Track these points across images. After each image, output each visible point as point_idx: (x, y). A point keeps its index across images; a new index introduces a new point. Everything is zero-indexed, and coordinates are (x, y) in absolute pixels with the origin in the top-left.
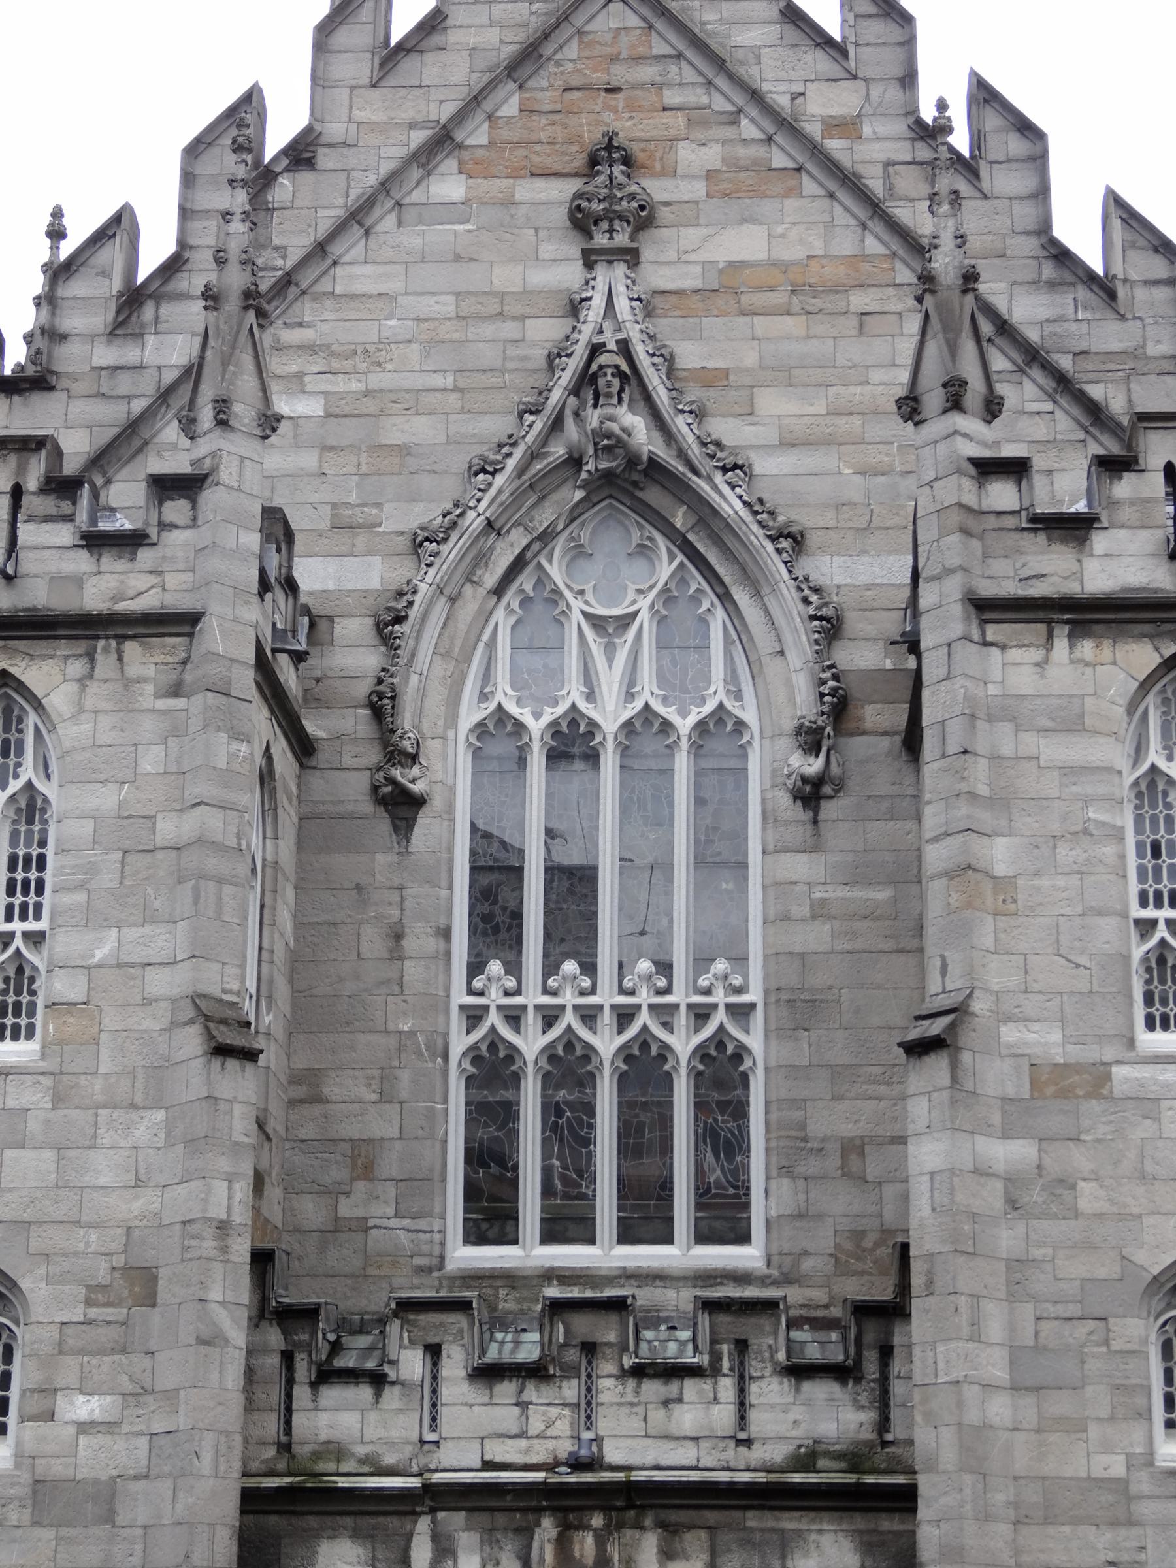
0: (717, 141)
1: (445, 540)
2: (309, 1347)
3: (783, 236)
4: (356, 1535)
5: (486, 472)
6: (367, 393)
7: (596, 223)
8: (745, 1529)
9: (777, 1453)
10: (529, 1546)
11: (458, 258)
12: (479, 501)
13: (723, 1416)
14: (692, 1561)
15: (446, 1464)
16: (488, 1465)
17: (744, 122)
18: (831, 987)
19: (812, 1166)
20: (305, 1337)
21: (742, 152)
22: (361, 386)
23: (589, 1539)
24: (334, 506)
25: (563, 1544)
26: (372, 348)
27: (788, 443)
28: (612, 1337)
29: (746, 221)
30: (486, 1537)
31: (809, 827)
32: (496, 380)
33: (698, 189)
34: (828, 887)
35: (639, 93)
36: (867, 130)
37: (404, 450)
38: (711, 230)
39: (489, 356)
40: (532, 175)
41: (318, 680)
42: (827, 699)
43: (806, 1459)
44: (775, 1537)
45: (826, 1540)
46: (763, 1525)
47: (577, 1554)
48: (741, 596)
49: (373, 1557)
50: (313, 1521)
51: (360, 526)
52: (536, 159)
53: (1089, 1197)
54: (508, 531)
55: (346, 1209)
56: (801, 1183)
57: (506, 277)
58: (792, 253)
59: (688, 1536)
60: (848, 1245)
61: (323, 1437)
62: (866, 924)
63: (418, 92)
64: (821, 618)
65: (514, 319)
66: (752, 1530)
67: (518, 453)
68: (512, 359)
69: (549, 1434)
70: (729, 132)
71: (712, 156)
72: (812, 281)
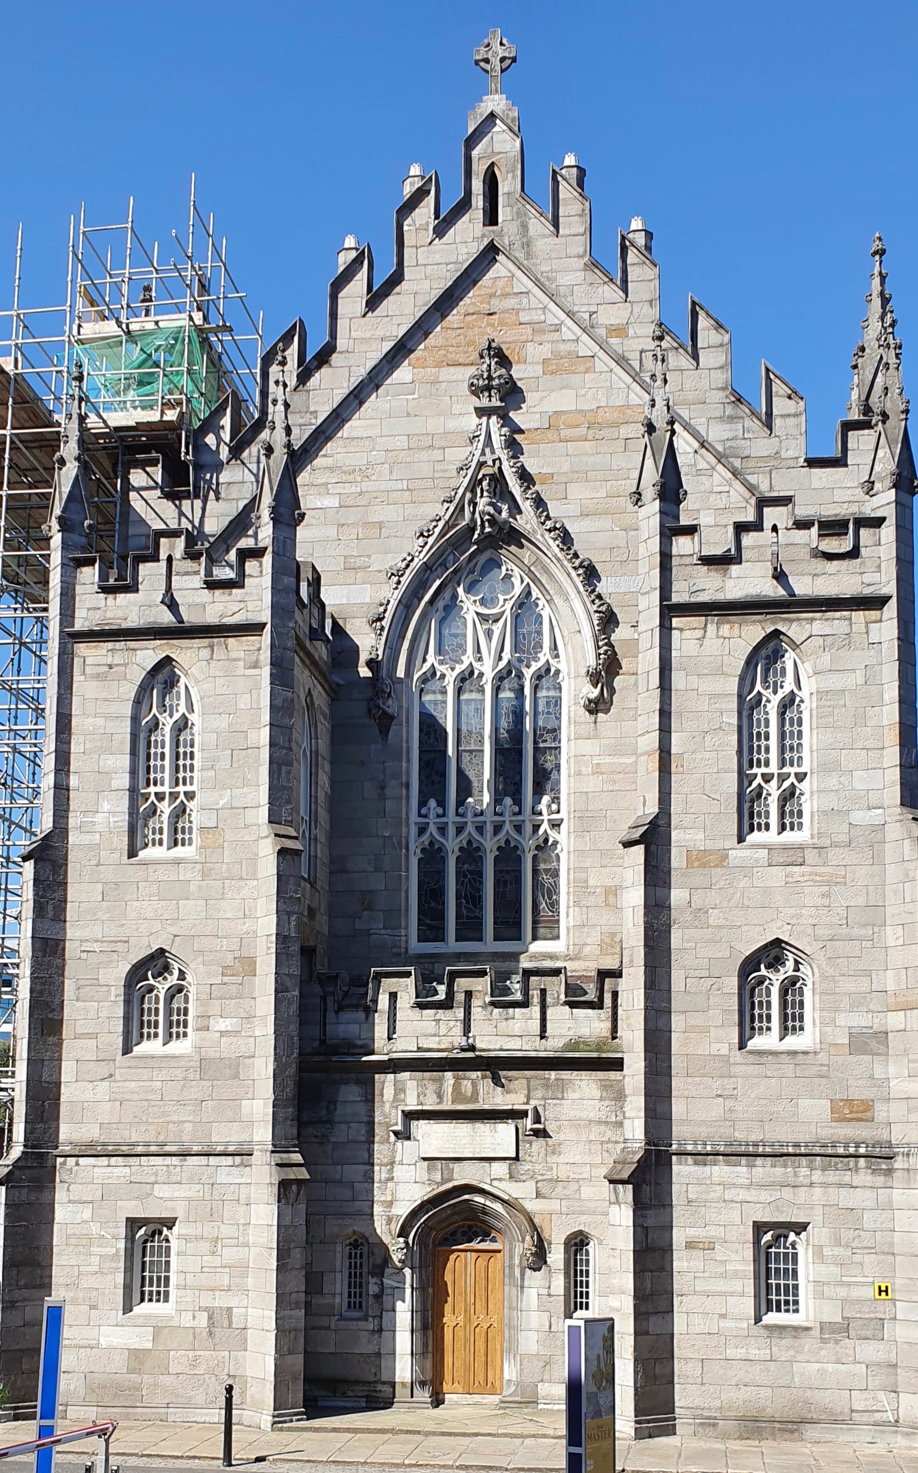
0: (548, 342)
1: (402, 575)
2: (333, 994)
3: (584, 395)
5: (424, 536)
6: (361, 493)
7: (482, 392)
9: (559, 1043)
11: (408, 415)
12: (420, 552)
13: (535, 1026)
15: (400, 1049)
16: (420, 1049)
17: (564, 329)
18: (601, 810)
19: (592, 900)
20: (331, 989)
21: (562, 347)
22: (359, 490)
24: (345, 557)
25: (456, 1087)
26: (364, 468)
27: (584, 515)
28: (480, 988)
29: (564, 387)
31: (593, 725)
32: (430, 484)
33: (539, 369)
34: (602, 757)
35: (507, 315)
36: (631, 332)
37: (381, 525)
38: (545, 394)
39: (426, 470)
40: (448, 365)
41: (339, 653)
42: (602, 656)
43: (573, 1045)
47: (463, 1091)
48: (558, 600)
51: (359, 568)
52: (450, 356)
53: (714, 918)
54: (436, 569)
55: (359, 925)
56: (584, 909)
57: (434, 425)
58: (588, 405)
60: (608, 940)
61: (341, 1036)
62: (621, 776)
63: (385, 319)
64: (600, 612)
65: (439, 448)
67: (441, 524)
68: (438, 471)
69: (449, 1034)
70: (555, 336)
71: (545, 351)
72: (600, 421)
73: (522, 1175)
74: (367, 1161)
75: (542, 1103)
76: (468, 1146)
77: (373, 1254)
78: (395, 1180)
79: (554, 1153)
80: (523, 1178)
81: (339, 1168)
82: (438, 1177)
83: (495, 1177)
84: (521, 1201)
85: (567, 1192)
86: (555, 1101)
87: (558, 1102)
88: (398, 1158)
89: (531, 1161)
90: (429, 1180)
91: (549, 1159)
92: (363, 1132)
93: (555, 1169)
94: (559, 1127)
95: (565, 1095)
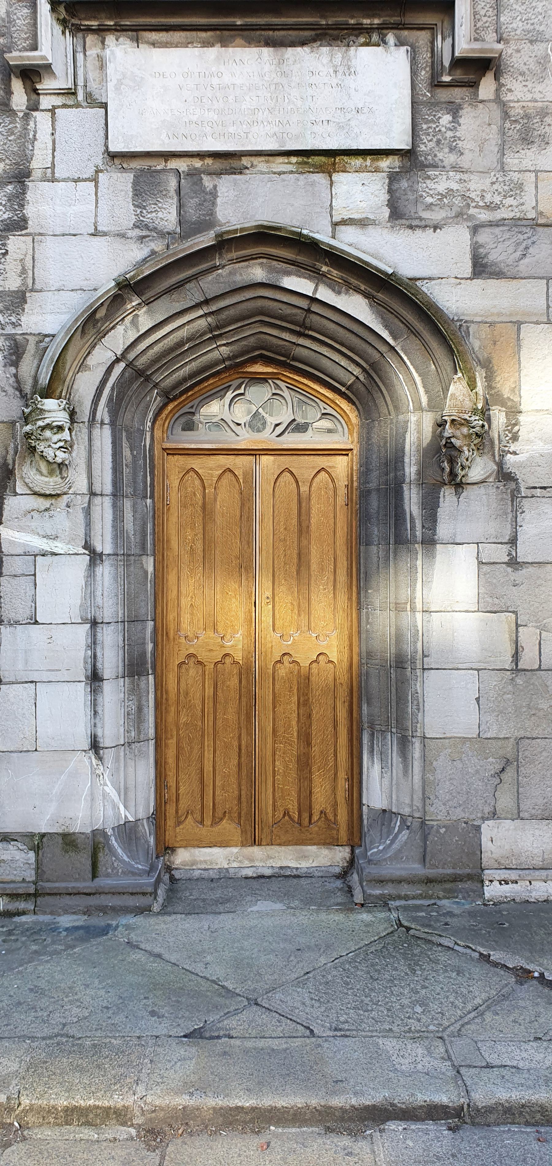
73: (429, 207)
76: (260, 116)
80: (437, 216)
91: (512, 160)
93: (530, 188)
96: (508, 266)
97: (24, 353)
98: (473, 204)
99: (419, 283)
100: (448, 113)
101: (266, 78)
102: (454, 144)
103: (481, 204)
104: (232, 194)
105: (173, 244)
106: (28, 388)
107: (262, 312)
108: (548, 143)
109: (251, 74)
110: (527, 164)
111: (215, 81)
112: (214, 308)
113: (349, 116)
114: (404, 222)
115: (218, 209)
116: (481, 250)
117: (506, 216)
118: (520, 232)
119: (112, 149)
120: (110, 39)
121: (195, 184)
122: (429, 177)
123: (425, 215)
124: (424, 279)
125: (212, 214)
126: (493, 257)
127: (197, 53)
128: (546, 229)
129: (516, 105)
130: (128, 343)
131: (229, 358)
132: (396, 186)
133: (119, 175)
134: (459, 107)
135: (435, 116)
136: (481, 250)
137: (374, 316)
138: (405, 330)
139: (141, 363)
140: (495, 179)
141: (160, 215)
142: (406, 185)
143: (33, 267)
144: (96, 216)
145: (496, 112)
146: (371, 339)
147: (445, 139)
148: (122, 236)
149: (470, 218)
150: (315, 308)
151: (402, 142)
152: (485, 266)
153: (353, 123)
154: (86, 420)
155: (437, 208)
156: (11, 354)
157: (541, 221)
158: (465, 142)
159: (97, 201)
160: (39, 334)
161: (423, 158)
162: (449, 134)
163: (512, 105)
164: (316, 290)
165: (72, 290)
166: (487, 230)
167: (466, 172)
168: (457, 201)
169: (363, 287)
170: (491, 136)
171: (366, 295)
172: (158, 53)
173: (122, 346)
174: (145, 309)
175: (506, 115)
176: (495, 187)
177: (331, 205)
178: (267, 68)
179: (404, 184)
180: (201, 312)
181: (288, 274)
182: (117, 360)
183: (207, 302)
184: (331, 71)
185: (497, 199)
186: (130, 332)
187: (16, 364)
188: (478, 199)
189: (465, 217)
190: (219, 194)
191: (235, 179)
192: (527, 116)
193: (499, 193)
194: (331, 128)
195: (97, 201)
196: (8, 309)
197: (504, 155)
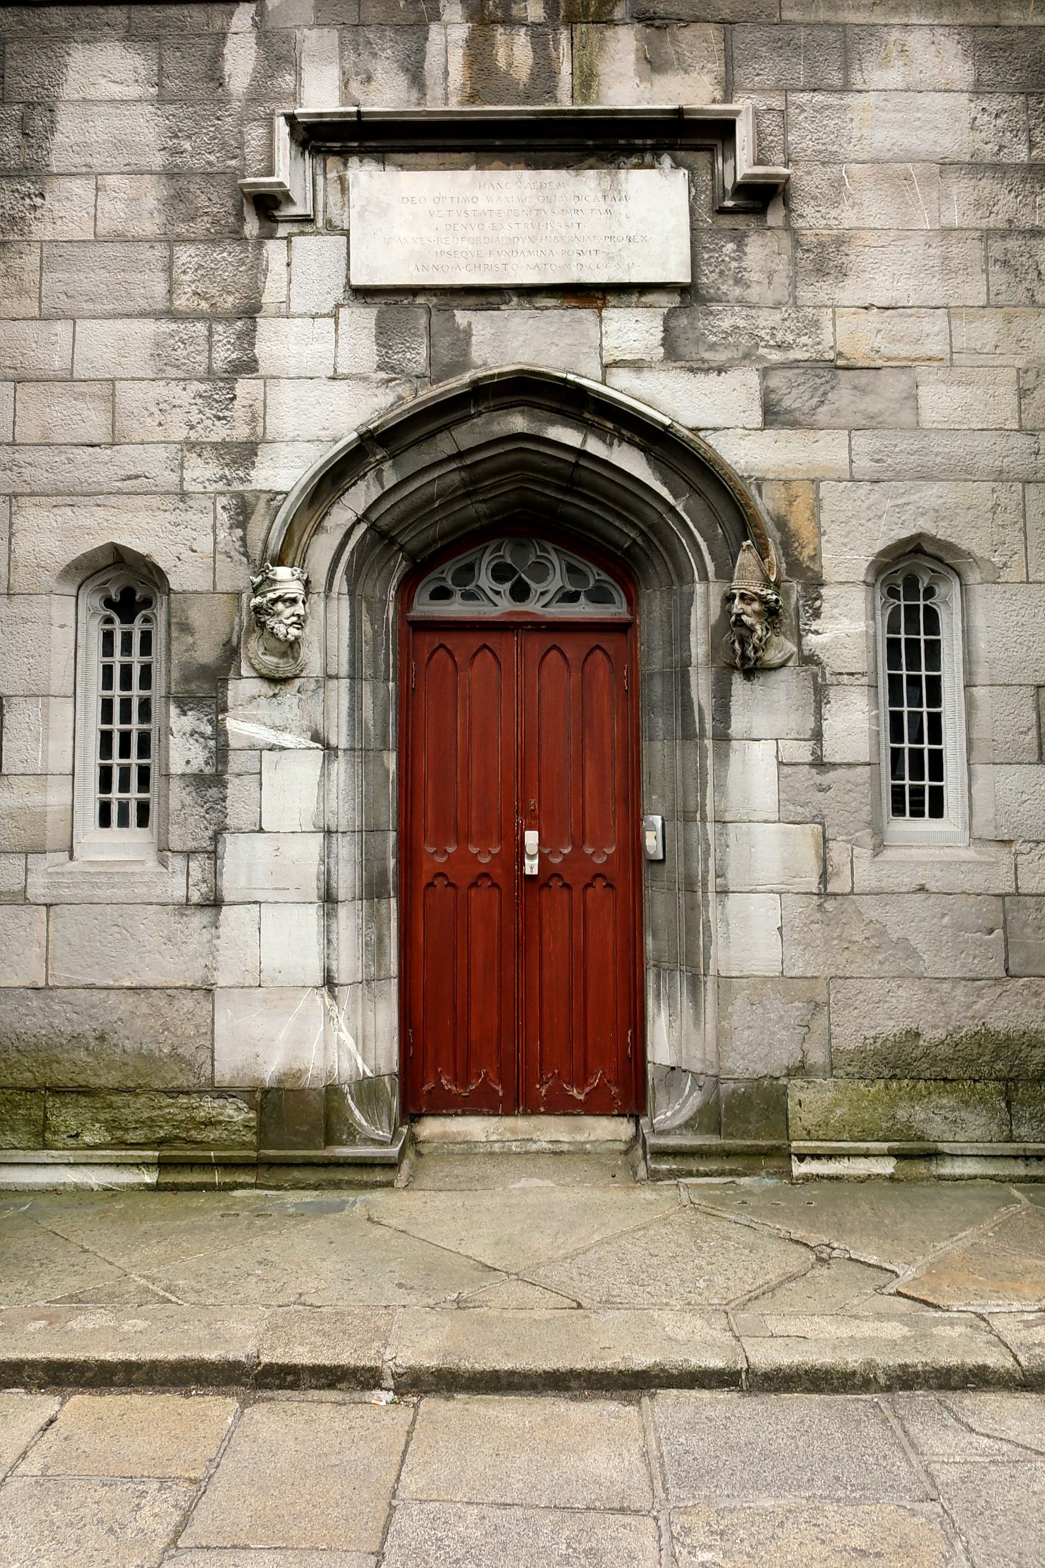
4: (130, 36)
8: (782, 22)
10: (421, 51)
14: (695, 75)
23: (522, 39)
30: (349, 36)
44: (832, 36)
45: (916, 41)
46: (811, 18)
47: (502, 63)
49: (161, 69)
50: (57, 16)
59: (687, 35)
66: (793, 24)
73: (712, 347)
74: (161, 305)
75: (777, 102)
76: (520, 246)
77: (186, 628)
78: (264, 368)
79: (821, 270)
81: (62, 328)
82: (417, 357)
83: (618, 356)
84: (712, 439)
85: (871, 405)
86: (819, 98)
87: (832, 99)
88: (272, 293)
89: (741, 302)
90: (380, 368)
91: (805, 294)
92: (150, 202)
94: (837, 185)
95: (856, 77)
96: (803, 414)
97: (252, 513)
98: (763, 344)
99: (702, 434)
100: (732, 241)
101: (526, 204)
102: (740, 275)
103: (772, 343)
104: (489, 331)
105: (423, 389)
106: (256, 552)
107: (522, 465)
108: (846, 275)
109: (510, 199)
110: (823, 297)
111: (470, 207)
112: (468, 461)
113: (619, 245)
114: (683, 363)
115: (474, 348)
116: (773, 396)
117: (799, 357)
118: (817, 376)
119: (355, 281)
120: (354, 161)
121: (447, 320)
122: (711, 313)
123: (707, 355)
124: (707, 429)
125: (466, 355)
126: (787, 403)
127: (449, 177)
128: (846, 372)
129: (808, 232)
130: (371, 502)
131: (486, 516)
132: (673, 323)
133: (362, 310)
134: (745, 235)
135: (717, 244)
136: (773, 396)
137: (650, 471)
138: (688, 487)
139: (384, 523)
140: (786, 316)
141: (408, 355)
142: (686, 322)
143: (265, 414)
144: (336, 356)
145: (786, 241)
146: (648, 498)
147: (729, 270)
148: (365, 379)
149: (761, 358)
150: (583, 462)
151: (683, 276)
152: (777, 413)
153: (624, 254)
154: (322, 590)
155: (721, 348)
156: (238, 514)
157: (840, 363)
158: (752, 273)
159: (337, 342)
160: (270, 491)
161: (704, 292)
162: (734, 264)
163: (804, 232)
164: (584, 441)
165: (309, 441)
166: (779, 372)
167: (754, 307)
168: (744, 340)
169: (637, 439)
170: (781, 267)
171: (642, 449)
172: (407, 178)
173: (363, 505)
174: (390, 462)
175: (797, 244)
176: (787, 323)
177: (601, 345)
178: (528, 192)
179: (684, 321)
180: (454, 466)
181: (553, 423)
182: (358, 521)
183: (460, 455)
184: (600, 195)
185: (790, 338)
186: (373, 489)
187: (243, 525)
188: (768, 338)
189: (753, 358)
190: (474, 332)
191: (492, 316)
192: (822, 245)
193: (792, 331)
194: (600, 259)
195: (337, 342)
196: (235, 463)
197: (796, 287)
